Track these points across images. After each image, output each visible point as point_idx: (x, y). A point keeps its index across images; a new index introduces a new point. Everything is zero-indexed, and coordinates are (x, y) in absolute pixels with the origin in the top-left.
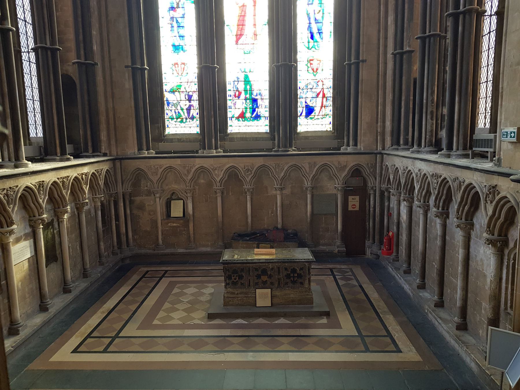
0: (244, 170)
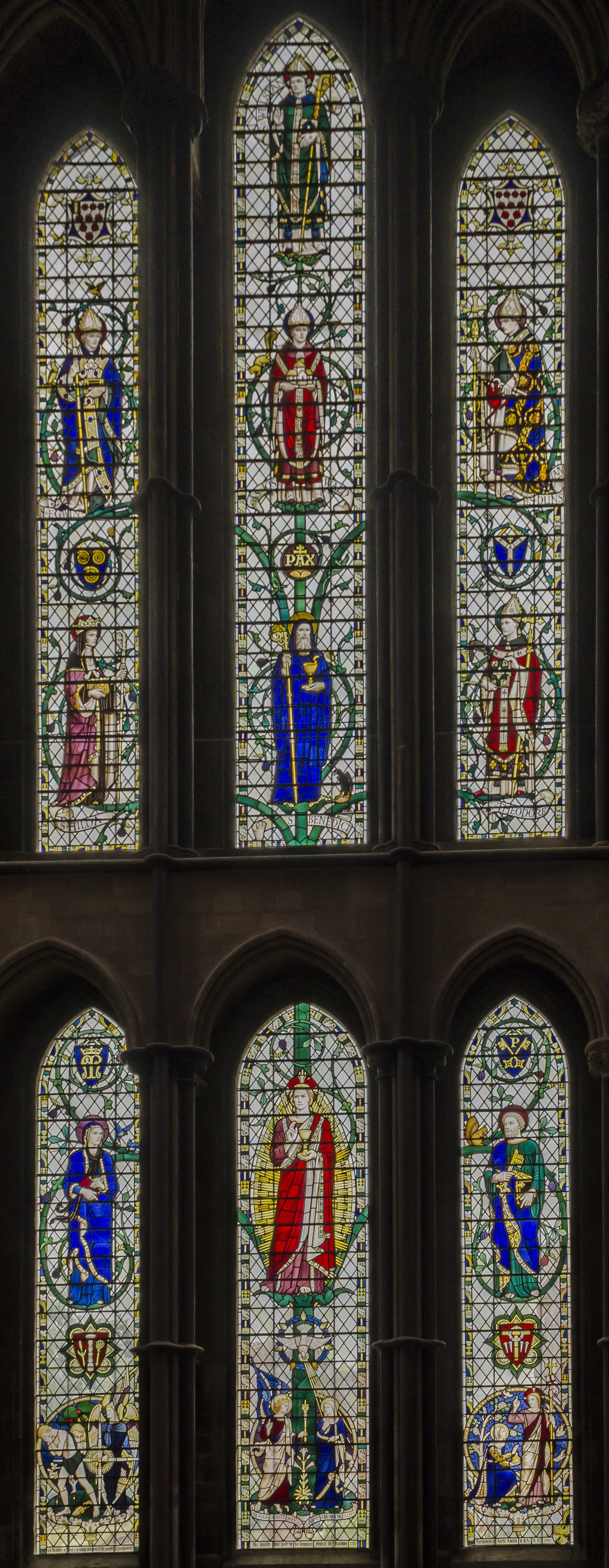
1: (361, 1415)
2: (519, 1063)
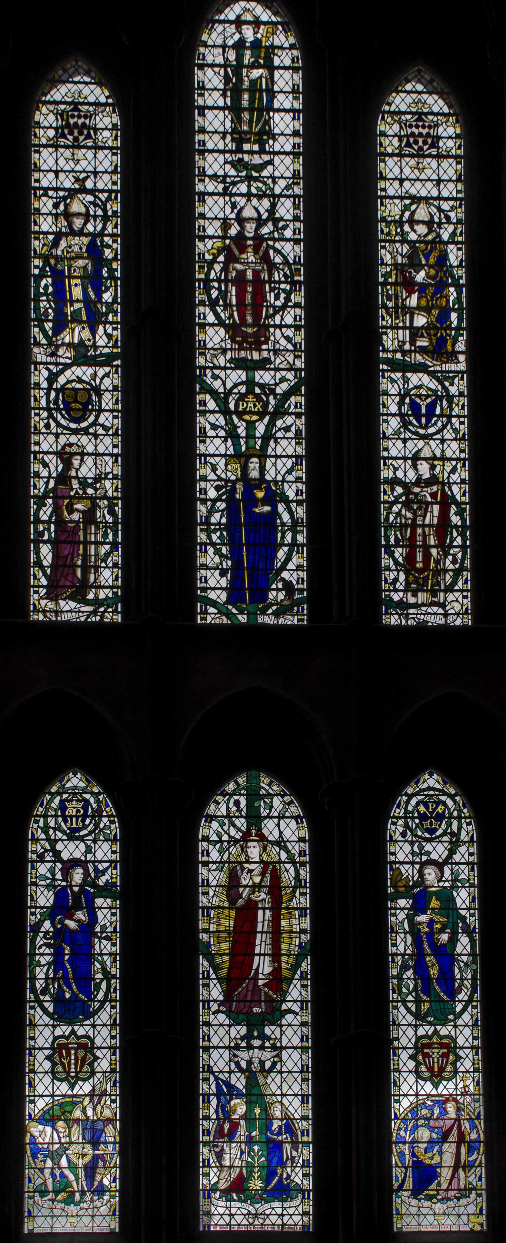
1: (304, 1118)
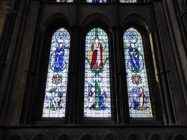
0: (96, 138)
2: (133, 37)
